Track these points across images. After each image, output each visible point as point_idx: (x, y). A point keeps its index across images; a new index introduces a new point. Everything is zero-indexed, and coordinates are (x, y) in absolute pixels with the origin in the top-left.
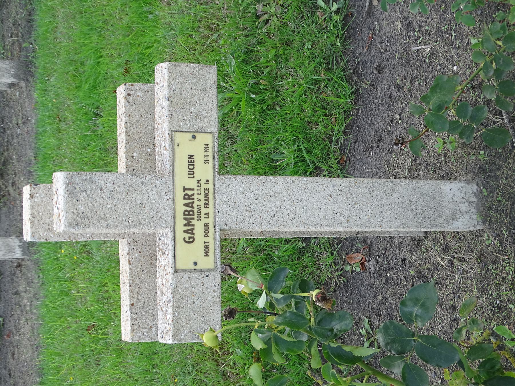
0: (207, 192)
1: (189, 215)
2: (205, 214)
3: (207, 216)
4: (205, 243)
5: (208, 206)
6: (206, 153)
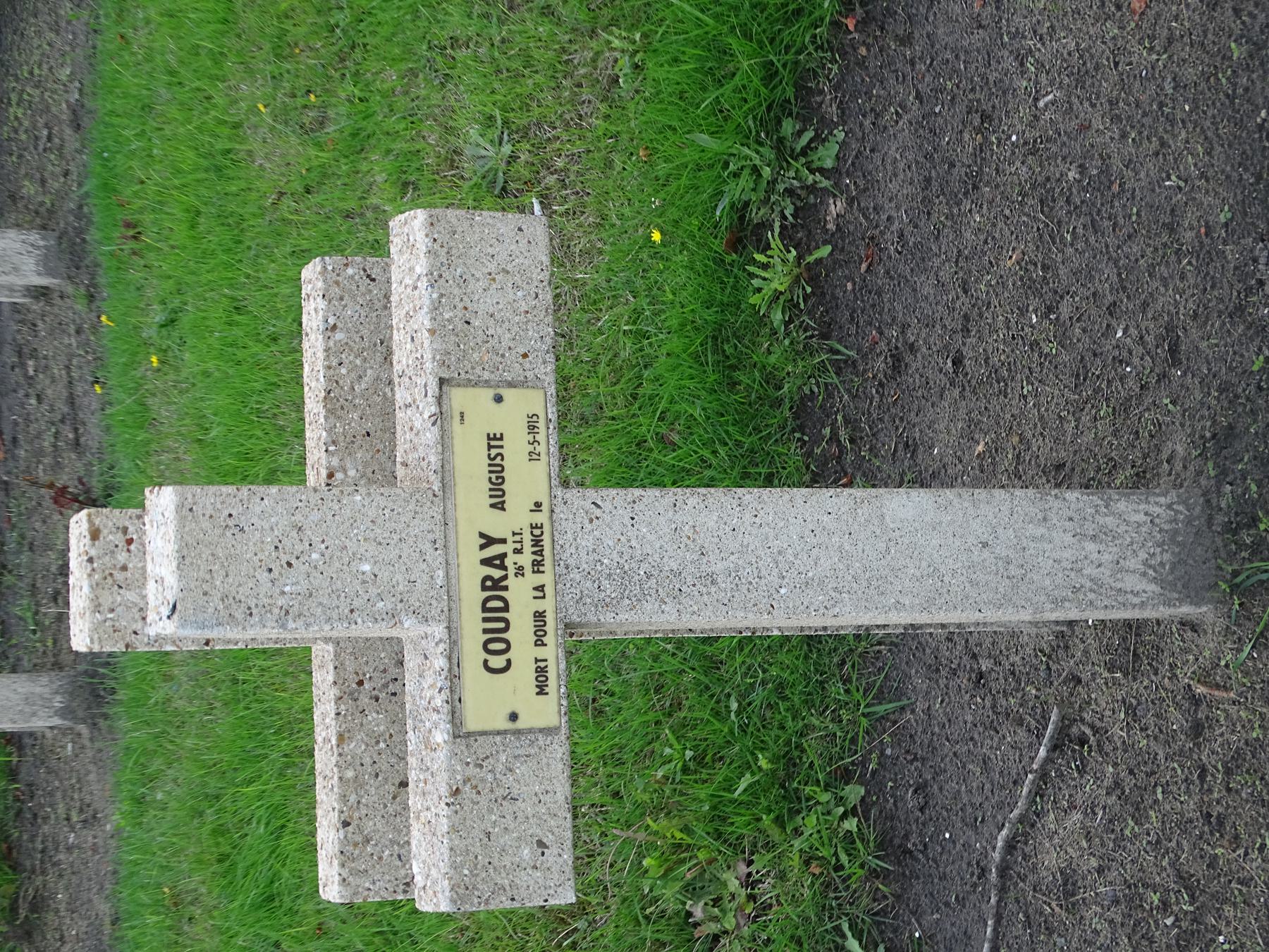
0: (537, 532)
2: (536, 589)
3: (541, 594)
4: (537, 660)
5: (541, 569)
6: (531, 438)
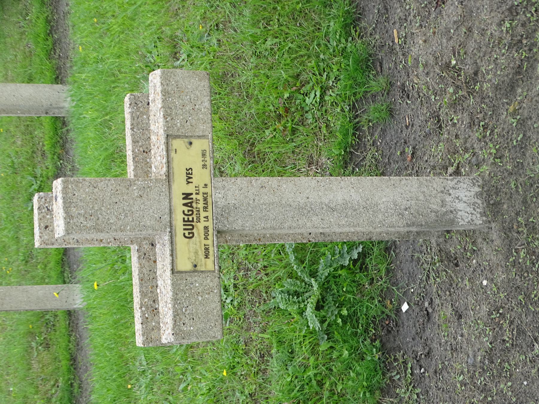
0: (205, 196)
1: (188, 221)
2: (204, 217)
3: (207, 220)
4: (205, 245)
6: (203, 159)
